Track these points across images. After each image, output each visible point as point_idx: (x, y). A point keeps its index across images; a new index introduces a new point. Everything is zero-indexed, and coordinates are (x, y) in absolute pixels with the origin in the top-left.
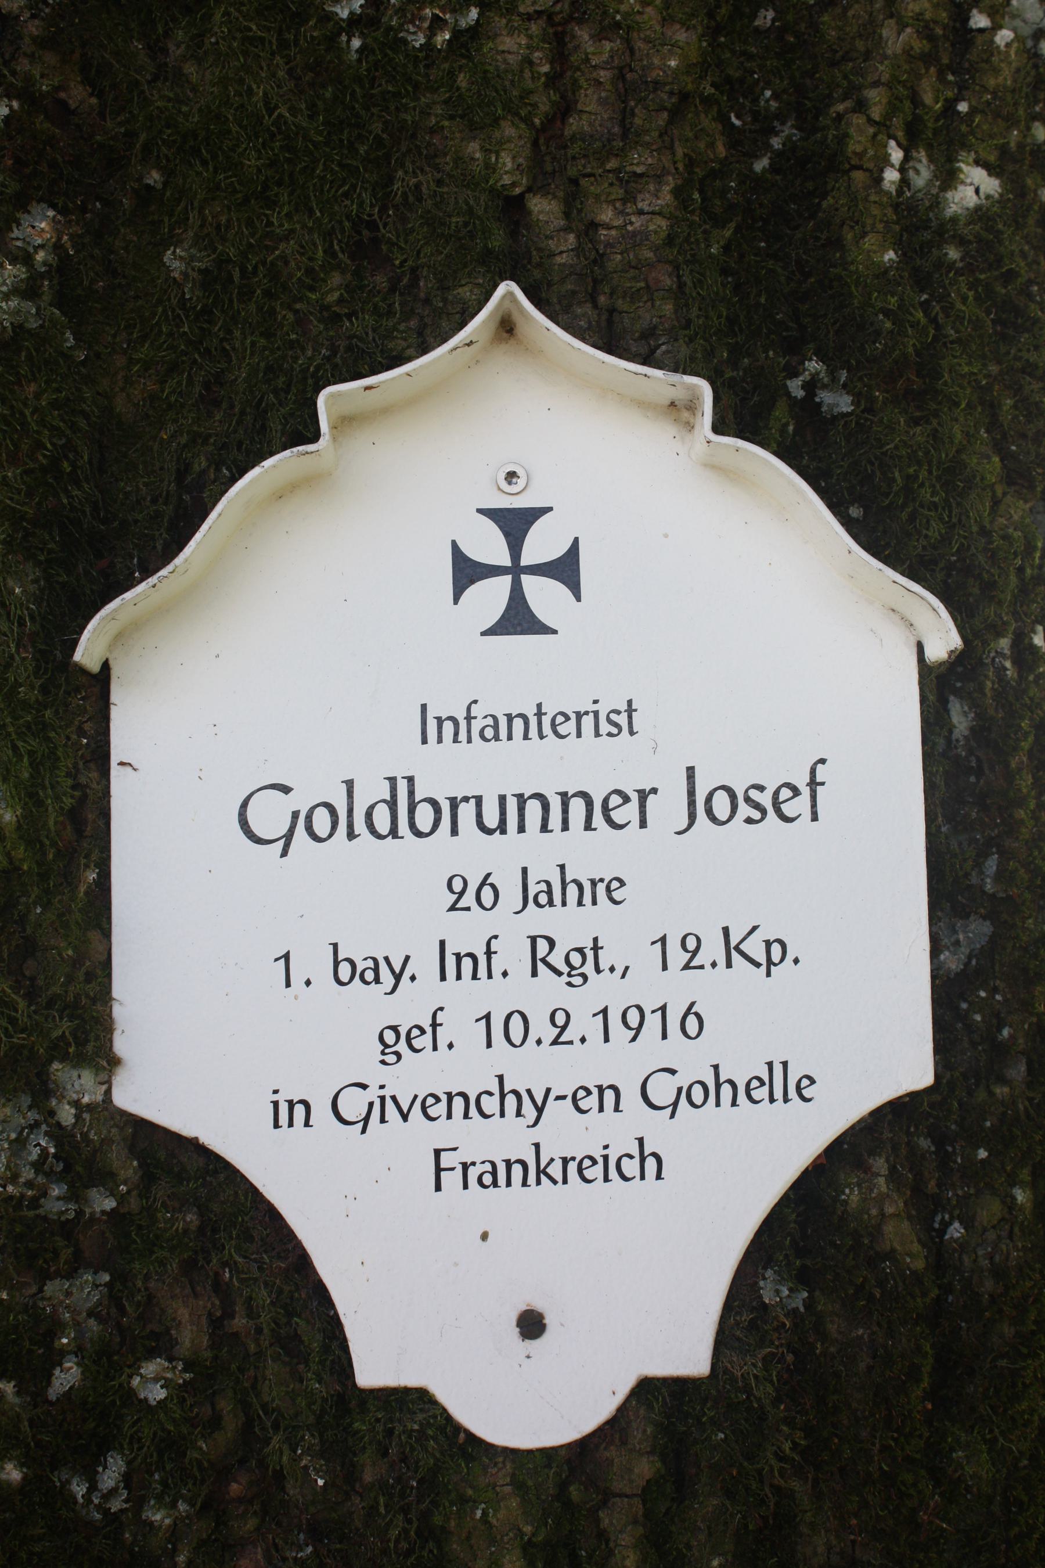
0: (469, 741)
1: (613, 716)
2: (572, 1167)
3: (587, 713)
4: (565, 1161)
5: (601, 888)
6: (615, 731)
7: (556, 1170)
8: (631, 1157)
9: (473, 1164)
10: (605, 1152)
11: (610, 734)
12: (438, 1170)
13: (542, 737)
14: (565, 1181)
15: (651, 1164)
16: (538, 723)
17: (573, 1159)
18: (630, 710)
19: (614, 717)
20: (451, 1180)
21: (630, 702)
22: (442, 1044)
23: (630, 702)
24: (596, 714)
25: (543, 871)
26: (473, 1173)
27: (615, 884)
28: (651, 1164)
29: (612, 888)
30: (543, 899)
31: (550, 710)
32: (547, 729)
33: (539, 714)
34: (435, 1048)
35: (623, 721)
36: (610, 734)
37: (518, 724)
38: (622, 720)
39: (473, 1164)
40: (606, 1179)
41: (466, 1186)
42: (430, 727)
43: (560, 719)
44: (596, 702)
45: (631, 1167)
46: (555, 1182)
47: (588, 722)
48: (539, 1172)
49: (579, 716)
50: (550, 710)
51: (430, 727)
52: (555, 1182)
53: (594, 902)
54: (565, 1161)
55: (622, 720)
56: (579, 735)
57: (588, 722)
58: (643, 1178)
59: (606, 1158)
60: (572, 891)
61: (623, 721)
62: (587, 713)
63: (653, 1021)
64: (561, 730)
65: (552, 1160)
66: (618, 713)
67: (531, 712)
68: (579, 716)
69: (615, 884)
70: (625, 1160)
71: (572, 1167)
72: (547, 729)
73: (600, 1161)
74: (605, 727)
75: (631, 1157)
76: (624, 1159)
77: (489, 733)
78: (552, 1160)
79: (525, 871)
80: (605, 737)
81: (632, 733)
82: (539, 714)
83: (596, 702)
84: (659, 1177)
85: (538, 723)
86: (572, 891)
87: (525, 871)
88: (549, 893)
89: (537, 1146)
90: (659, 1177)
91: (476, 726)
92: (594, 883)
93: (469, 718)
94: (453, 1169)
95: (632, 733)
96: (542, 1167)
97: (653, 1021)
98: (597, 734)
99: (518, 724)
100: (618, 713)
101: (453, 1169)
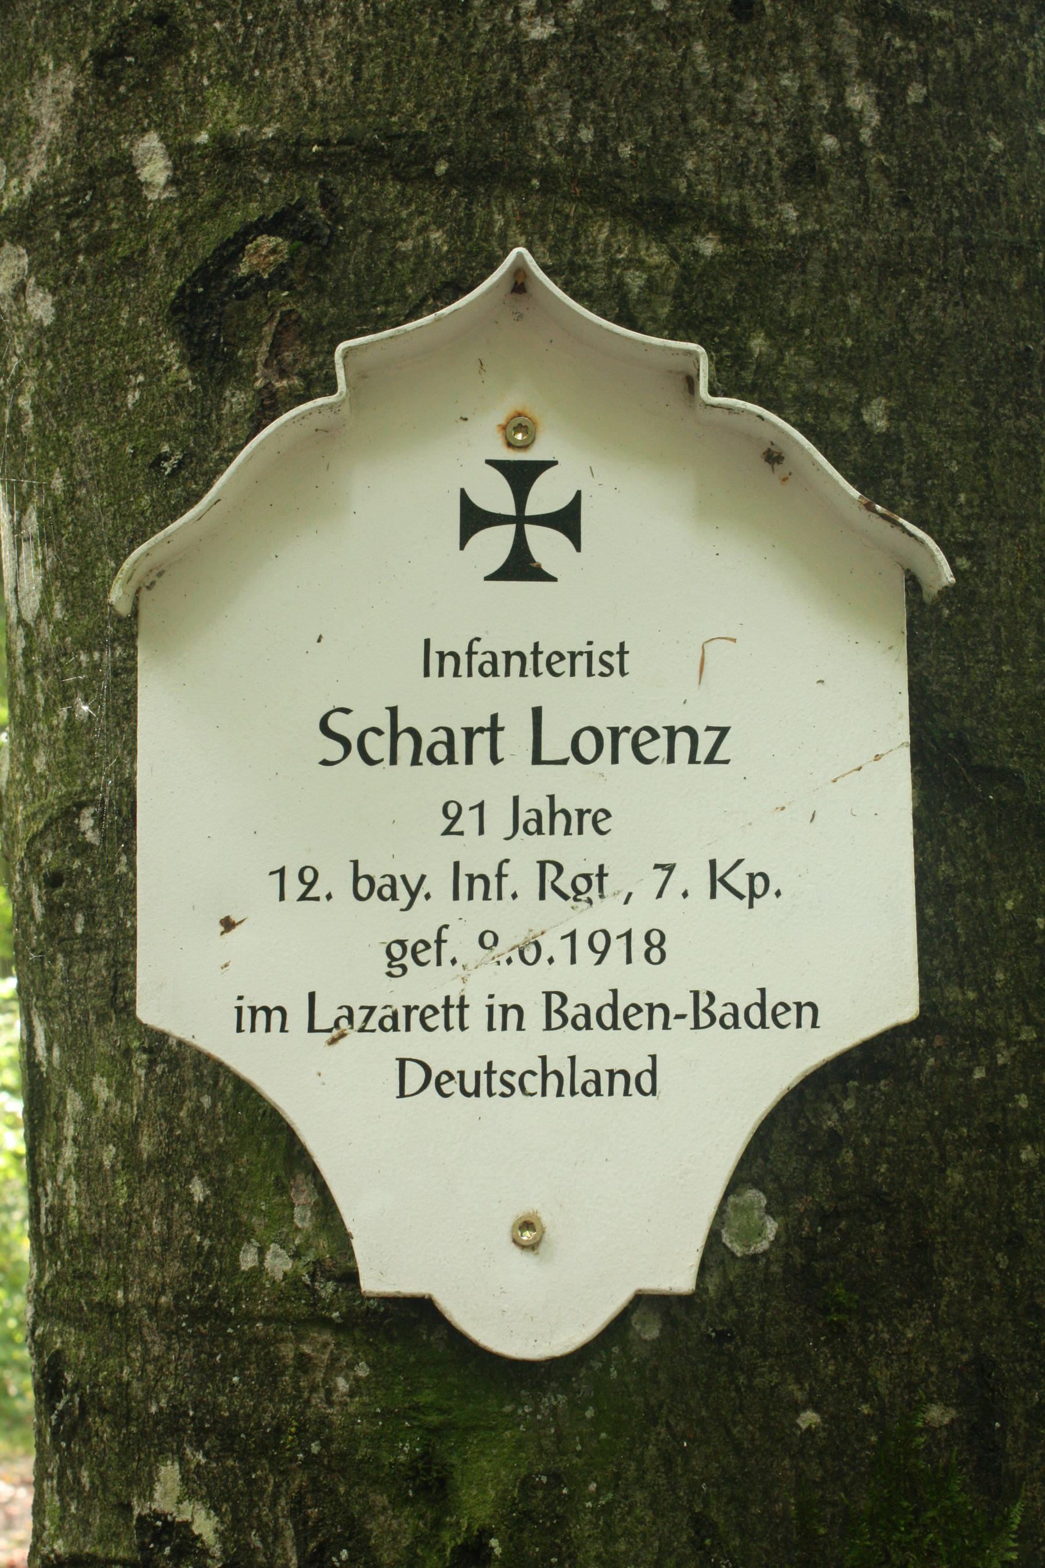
0: (470, 674)
1: (606, 658)
3: (581, 653)
5: (588, 819)
6: (607, 671)
11: (602, 674)
13: (537, 673)
16: (534, 661)
18: (622, 652)
19: (606, 658)
21: (622, 645)
23: (622, 645)
24: (590, 654)
25: (534, 800)
27: (601, 816)
29: (598, 820)
30: (532, 826)
32: (542, 667)
33: (536, 652)
35: (614, 662)
36: (602, 674)
37: (516, 661)
38: (614, 661)
42: (434, 660)
43: (555, 658)
44: (590, 643)
47: (581, 662)
49: (573, 656)
50: (546, 649)
51: (434, 660)
53: (580, 832)
55: (614, 661)
56: (573, 674)
57: (581, 662)
60: (560, 819)
61: (614, 662)
62: (581, 653)
64: (556, 668)
66: (610, 654)
67: (528, 651)
68: (573, 656)
69: (601, 816)
72: (542, 667)
74: (597, 668)
77: (488, 669)
79: (516, 800)
80: (597, 677)
81: (623, 673)
82: (536, 652)
83: (590, 643)
85: (534, 661)
86: (560, 819)
87: (516, 800)
88: (539, 821)
91: (477, 660)
92: (581, 813)
93: (470, 653)
95: (623, 673)
98: (590, 674)
99: (516, 661)
100: (610, 654)
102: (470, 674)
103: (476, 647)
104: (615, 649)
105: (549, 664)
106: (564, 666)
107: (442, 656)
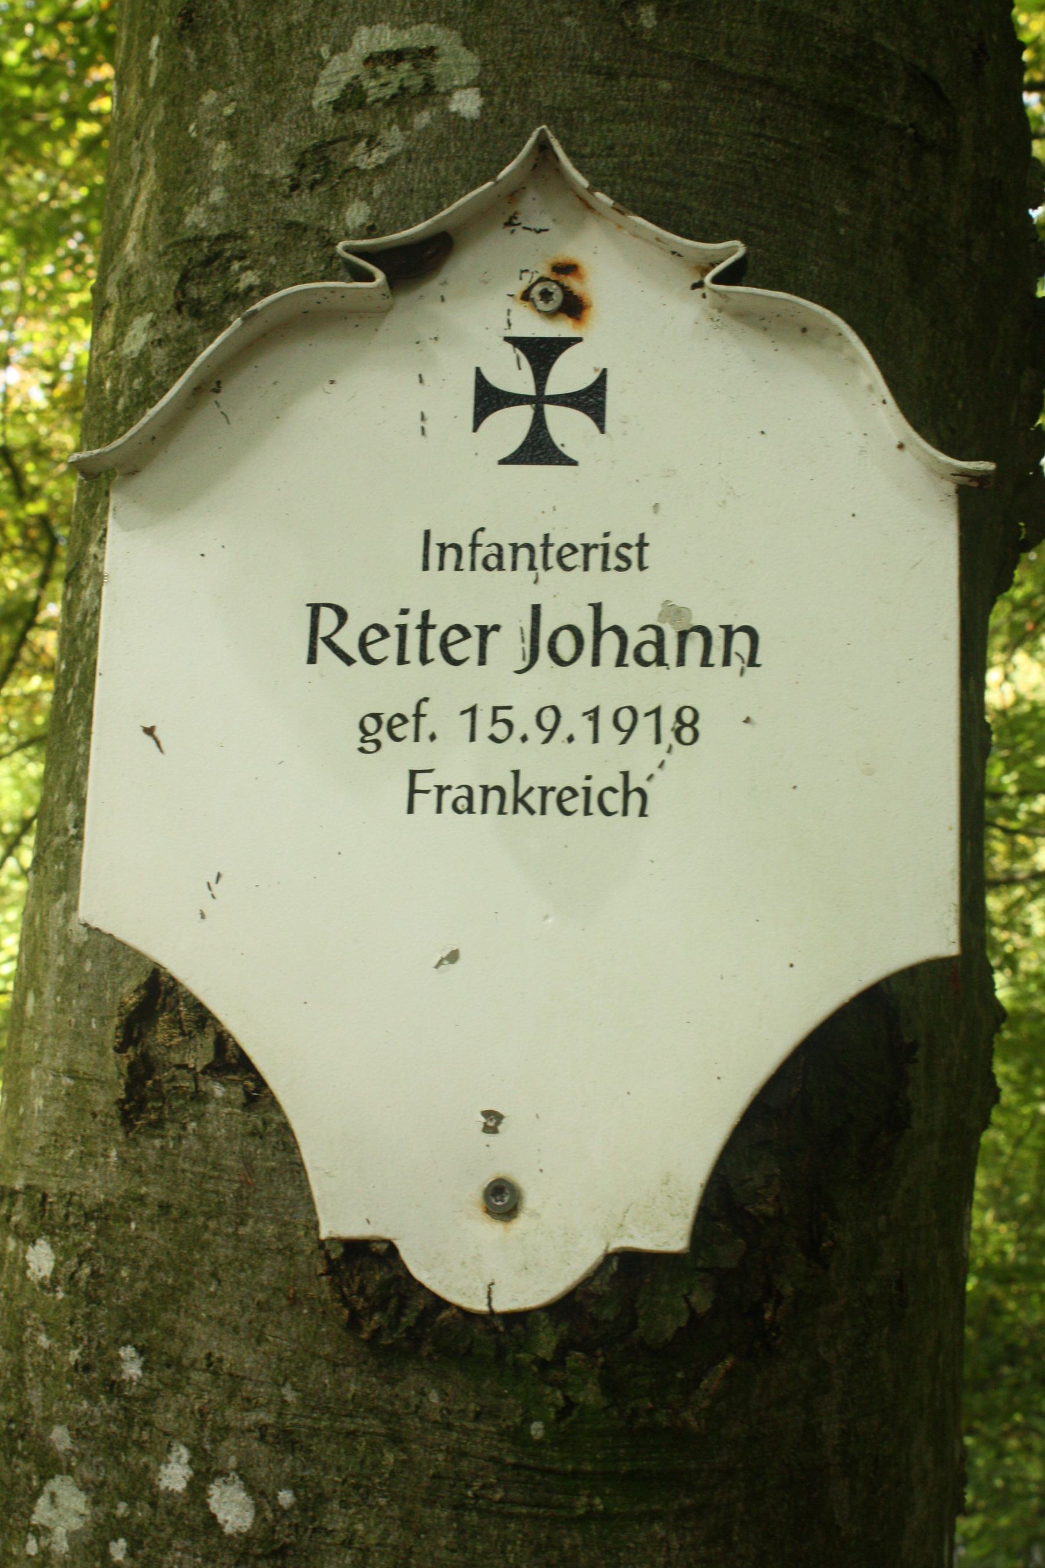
0: (473, 568)
2: (552, 797)
4: (545, 791)
6: (624, 565)
7: (534, 800)
8: (614, 790)
9: (449, 787)
10: (587, 783)
12: (413, 791)
14: (543, 812)
15: (635, 799)
16: (546, 555)
17: (553, 789)
18: (642, 545)
19: (624, 551)
20: (425, 803)
22: (424, 734)
24: (606, 547)
26: (448, 797)
28: (635, 799)
31: (558, 540)
34: (417, 739)
36: (619, 569)
38: (633, 554)
39: (449, 787)
40: (587, 812)
41: (439, 810)
42: (434, 552)
45: (613, 802)
46: (532, 812)
47: (596, 556)
48: (519, 800)
49: (587, 548)
51: (434, 552)
52: (532, 812)
54: (545, 791)
55: (633, 554)
57: (596, 556)
58: (625, 813)
59: (587, 790)
62: (596, 546)
63: (646, 725)
65: (531, 789)
67: (537, 542)
70: (608, 795)
71: (552, 797)
73: (582, 793)
74: (613, 561)
75: (614, 790)
76: (608, 795)
77: (493, 562)
78: (531, 789)
81: (642, 567)
82: (546, 545)
84: (642, 813)
89: (516, 773)
90: (642, 813)
91: (481, 554)
93: (474, 545)
94: (427, 792)
95: (642, 567)
96: (521, 792)
97: (646, 725)
98: (605, 568)
100: (628, 546)
101: (427, 792)
102: (473, 568)
103: (481, 538)
104: (634, 540)
105: (560, 558)
106: (577, 559)
107: (443, 547)
